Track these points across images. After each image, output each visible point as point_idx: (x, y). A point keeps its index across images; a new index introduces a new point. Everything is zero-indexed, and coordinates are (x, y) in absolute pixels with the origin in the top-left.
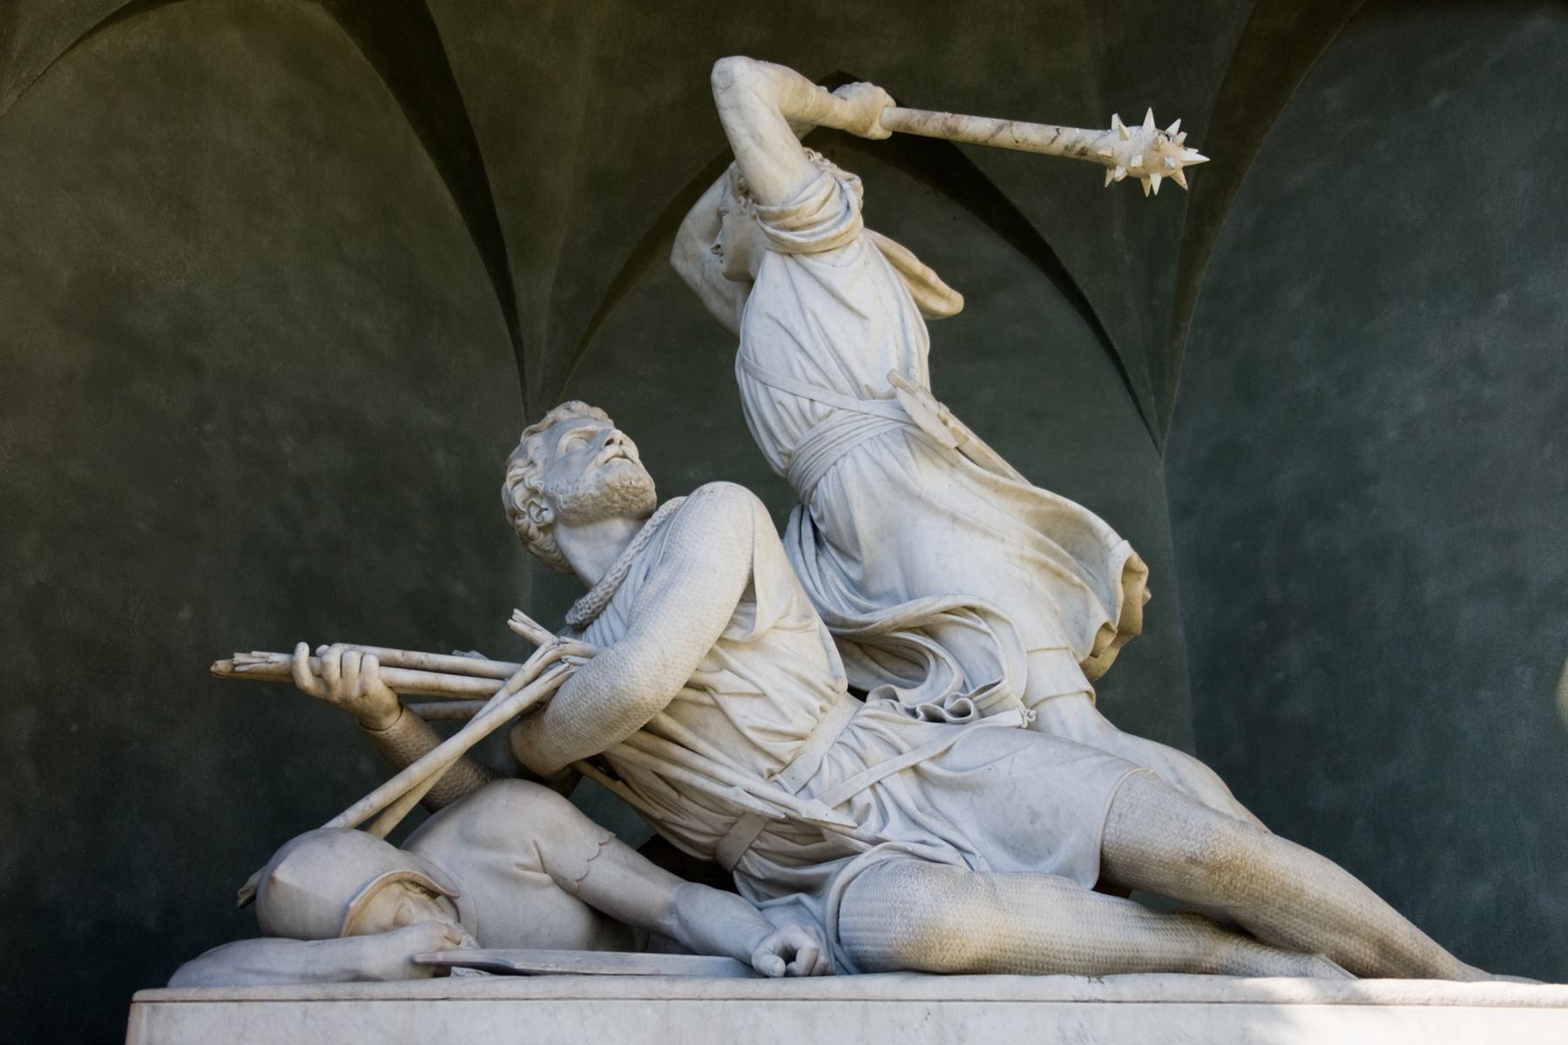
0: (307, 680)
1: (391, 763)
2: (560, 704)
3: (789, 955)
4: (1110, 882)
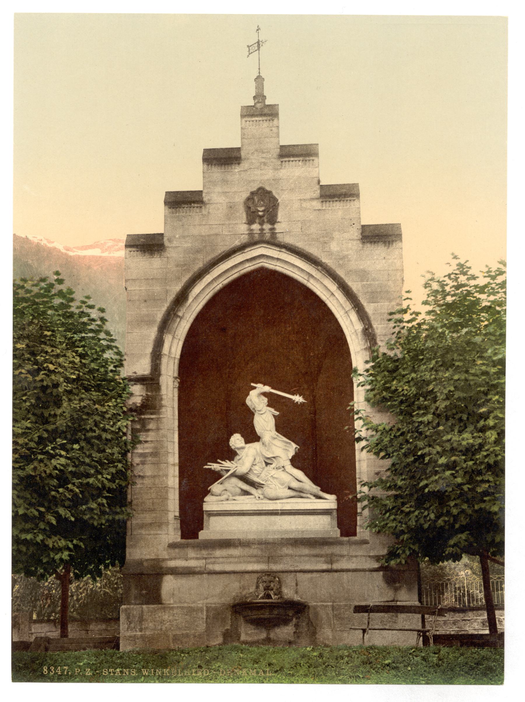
0: (213, 469)
1: (220, 476)
2: (237, 471)
3: (259, 498)
4: (290, 488)
